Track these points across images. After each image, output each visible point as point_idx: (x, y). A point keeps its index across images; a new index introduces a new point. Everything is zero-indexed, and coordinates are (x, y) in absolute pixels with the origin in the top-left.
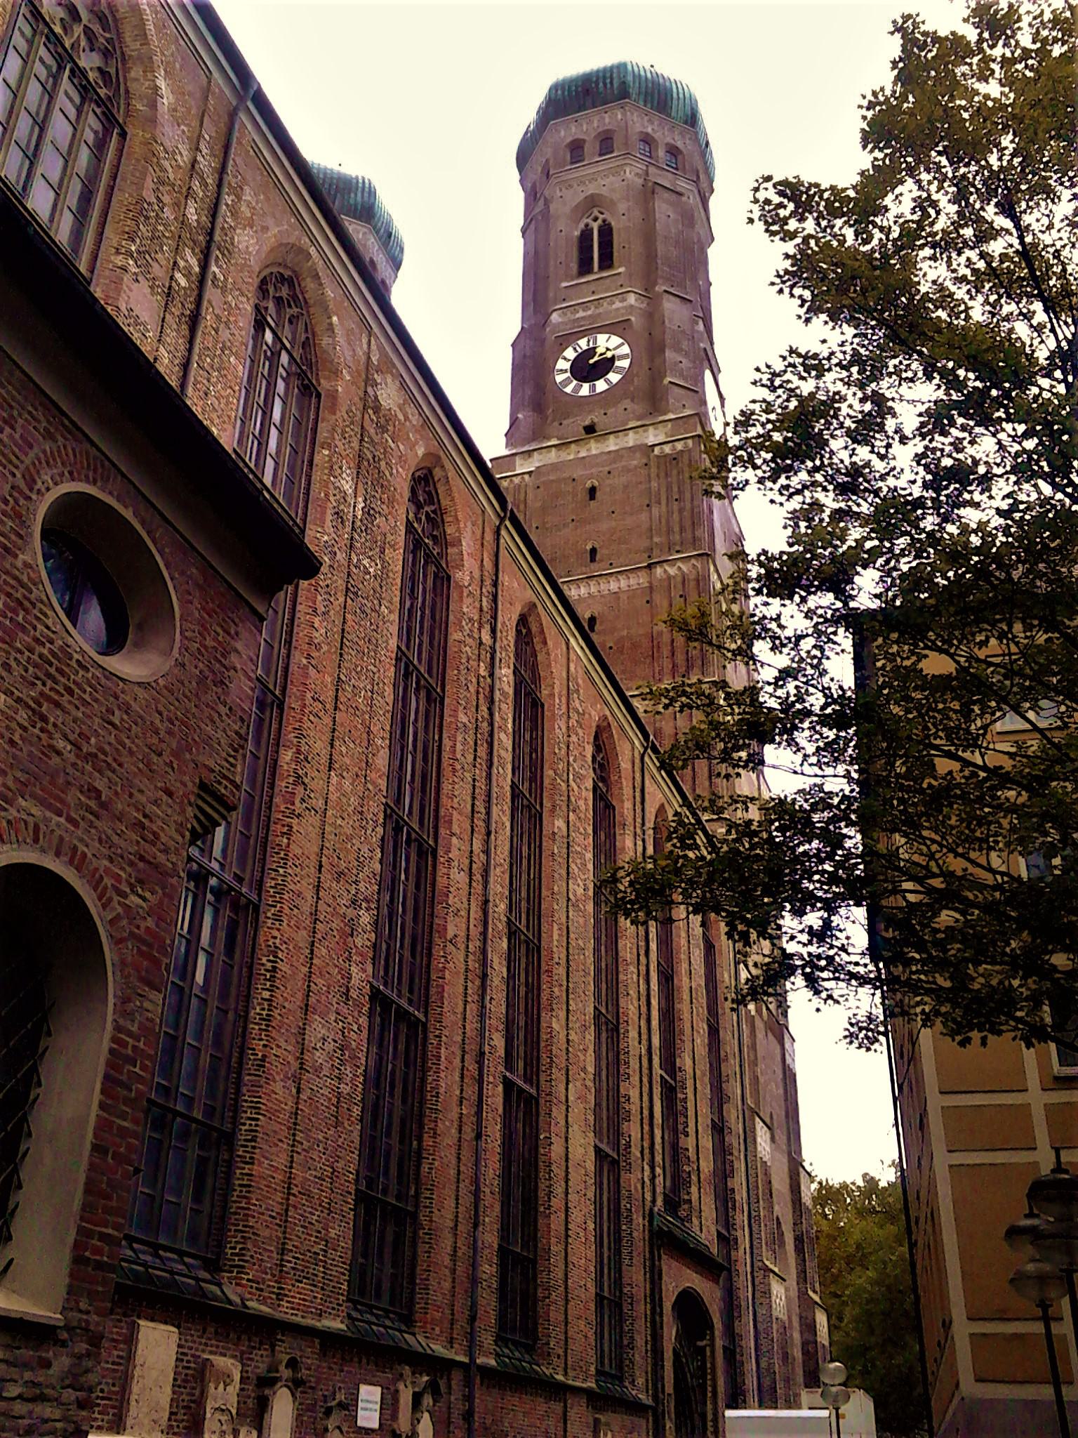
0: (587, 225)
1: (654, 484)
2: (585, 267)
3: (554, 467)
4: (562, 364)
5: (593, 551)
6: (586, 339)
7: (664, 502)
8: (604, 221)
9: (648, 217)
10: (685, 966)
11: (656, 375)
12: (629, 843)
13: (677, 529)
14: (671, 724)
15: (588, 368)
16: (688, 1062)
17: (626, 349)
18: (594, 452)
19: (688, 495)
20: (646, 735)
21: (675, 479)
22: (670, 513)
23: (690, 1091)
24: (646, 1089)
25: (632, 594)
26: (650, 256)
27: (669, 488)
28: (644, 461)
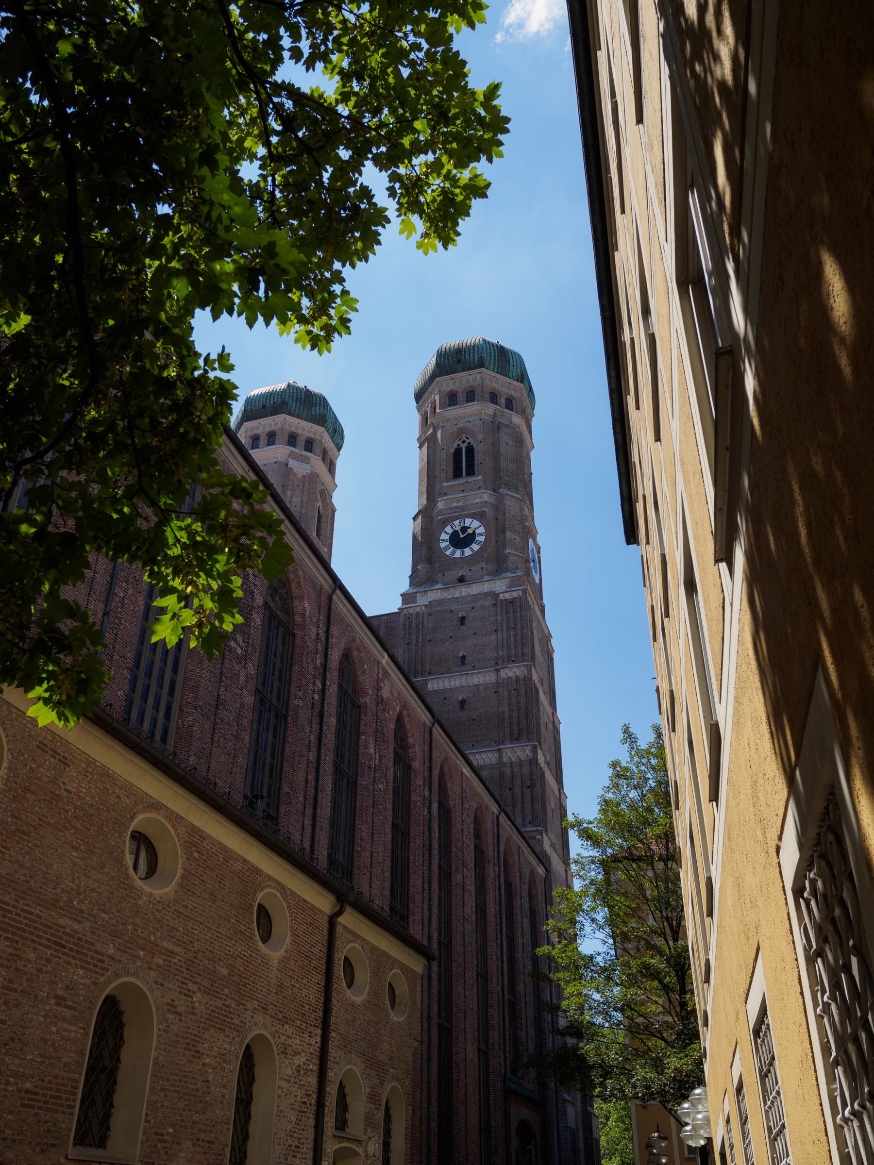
0: (459, 445)
1: (499, 618)
2: (457, 474)
3: (440, 602)
4: (444, 536)
5: (464, 658)
6: (458, 521)
7: (505, 629)
8: (469, 443)
9: (495, 444)
10: (520, 930)
11: (500, 546)
12: (491, 871)
13: (512, 646)
14: (509, 770)
15: (461, 540)
16: (522, 987)
17: (482, 530)
18: (464, 594)
19: (519, 626)
20: (500, 806)
21: (511, 615)
22: (509, 636)
23: (523, 1004)
24: (501, 1010)
25: (487, 686)
26: (497, 469)
27: (508, 620)
28: (494, 602)
